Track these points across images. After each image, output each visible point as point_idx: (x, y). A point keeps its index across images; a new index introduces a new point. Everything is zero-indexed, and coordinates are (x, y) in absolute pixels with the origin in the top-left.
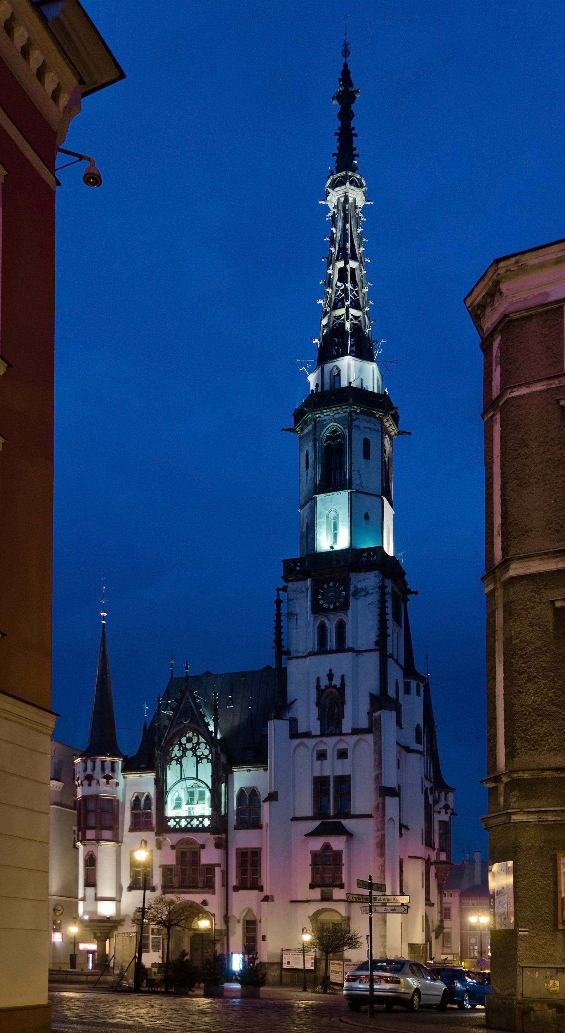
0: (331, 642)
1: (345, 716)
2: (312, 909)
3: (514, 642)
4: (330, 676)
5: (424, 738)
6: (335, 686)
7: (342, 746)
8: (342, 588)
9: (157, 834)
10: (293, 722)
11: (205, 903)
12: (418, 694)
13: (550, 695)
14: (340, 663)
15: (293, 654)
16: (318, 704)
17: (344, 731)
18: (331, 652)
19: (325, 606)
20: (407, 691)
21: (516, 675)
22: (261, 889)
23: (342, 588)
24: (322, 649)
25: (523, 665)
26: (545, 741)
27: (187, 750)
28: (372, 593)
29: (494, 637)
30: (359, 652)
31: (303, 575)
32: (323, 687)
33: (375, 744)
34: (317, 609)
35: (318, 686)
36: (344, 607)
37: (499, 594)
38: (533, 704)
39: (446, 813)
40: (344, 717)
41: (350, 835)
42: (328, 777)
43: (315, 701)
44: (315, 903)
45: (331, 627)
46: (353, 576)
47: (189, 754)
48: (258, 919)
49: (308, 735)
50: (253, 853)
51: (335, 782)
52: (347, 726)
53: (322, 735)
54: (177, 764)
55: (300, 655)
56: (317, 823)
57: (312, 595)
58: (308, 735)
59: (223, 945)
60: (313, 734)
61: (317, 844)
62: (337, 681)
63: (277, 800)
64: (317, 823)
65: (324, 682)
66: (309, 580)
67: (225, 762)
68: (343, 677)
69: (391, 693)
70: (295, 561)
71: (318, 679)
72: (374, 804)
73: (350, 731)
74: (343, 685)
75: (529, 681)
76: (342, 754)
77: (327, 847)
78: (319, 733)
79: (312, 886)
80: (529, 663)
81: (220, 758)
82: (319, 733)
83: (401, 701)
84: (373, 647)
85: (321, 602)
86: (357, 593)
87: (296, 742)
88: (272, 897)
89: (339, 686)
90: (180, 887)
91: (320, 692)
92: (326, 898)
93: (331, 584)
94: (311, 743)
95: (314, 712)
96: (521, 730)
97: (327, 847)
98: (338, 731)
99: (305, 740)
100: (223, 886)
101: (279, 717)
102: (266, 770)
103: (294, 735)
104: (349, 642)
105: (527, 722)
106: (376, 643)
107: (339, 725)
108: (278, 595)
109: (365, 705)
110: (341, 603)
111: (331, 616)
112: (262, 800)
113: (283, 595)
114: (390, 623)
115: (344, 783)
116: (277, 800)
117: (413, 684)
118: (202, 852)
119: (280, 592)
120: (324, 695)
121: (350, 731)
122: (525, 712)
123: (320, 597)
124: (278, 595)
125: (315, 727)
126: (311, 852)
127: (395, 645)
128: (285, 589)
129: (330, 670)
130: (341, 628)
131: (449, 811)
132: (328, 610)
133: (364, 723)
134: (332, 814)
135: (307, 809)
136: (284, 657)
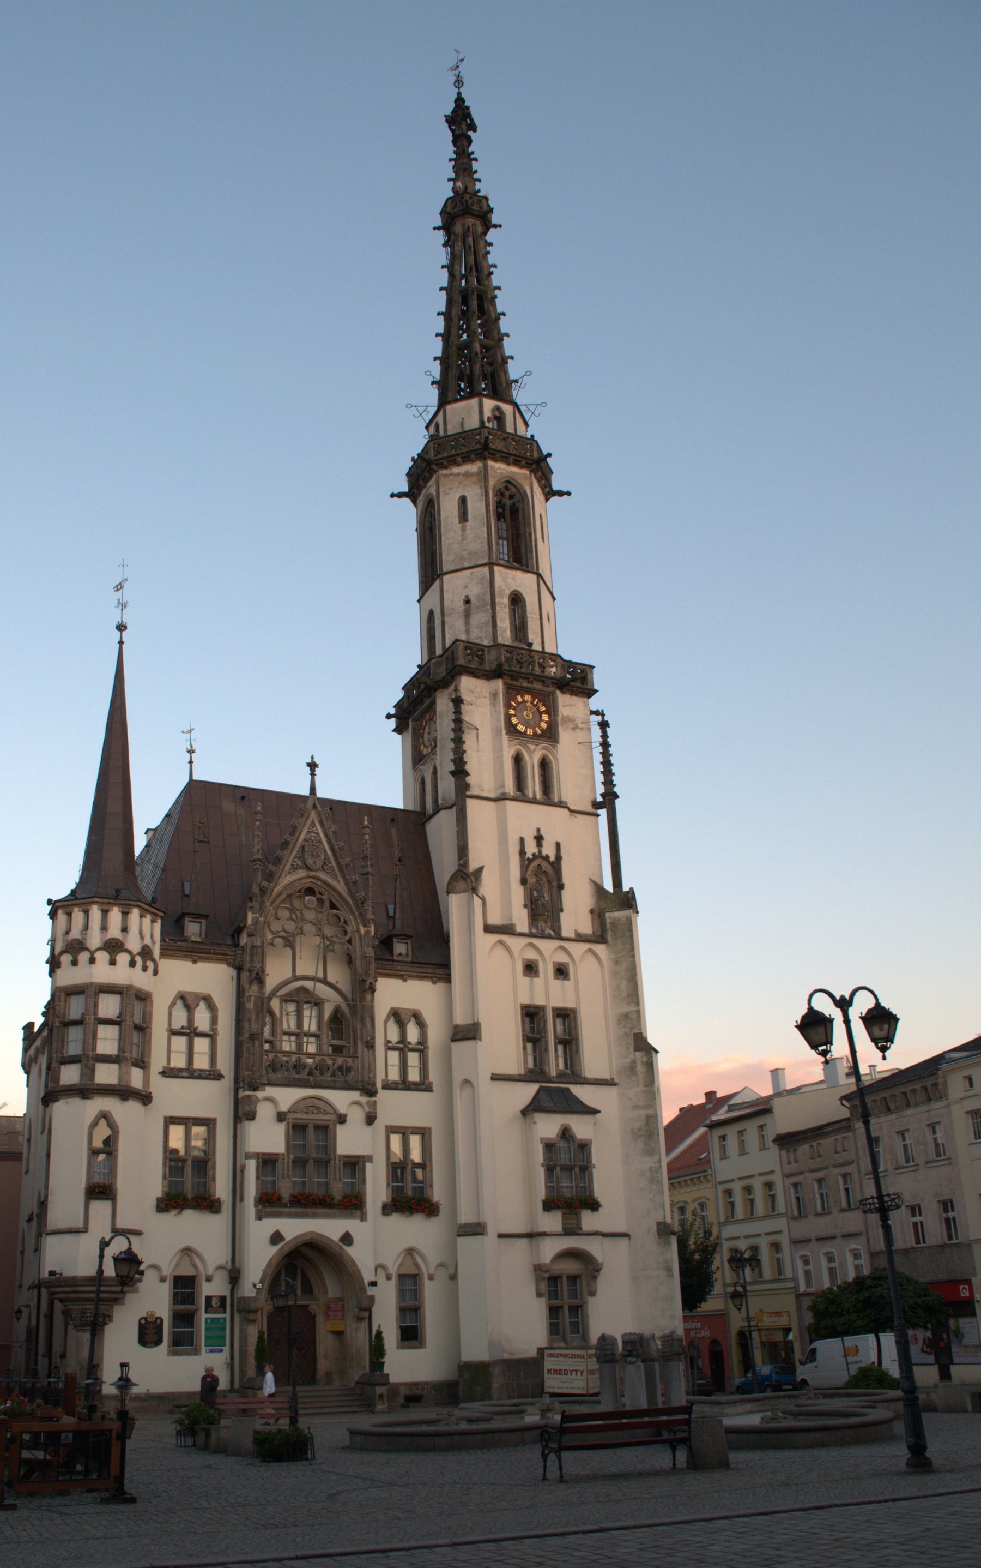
0: (534, 786)
1: (564, 907)
2: (549, 1249)
4: (539, 839)
6: (547, 858)
7: (562, 958)
11: (347, 1239)
16: (524, 881)
17: (564, 934)
18: (534, 801)
24: (521, 794)
28: (582, 729)
30: (571, 811)
32: (529, 855)
33: (616, 962)
34: (512, 730)
35: (522, 852)
36: (550, 735)
40: (562, 910)
44: (554, 1238)
49: (507, 930)
53: (531, 935)
54: (286, 946)
55: (485, 794)
56: (531, 1089)
58: (507, 930)
61: (548, 1126)
64: (533, 1088)
68: (558, 845)
71: (522, 840)
74: (559, 858)
76: (561, 972)
77: (566, 1133)
79: (548, 1206)
82: (526, 930)
85: (514, 720)
89: (552, 858)
91: (525, 862)
92: (571, 1230)
93: (528, 698)
94: (516, 944)
95: (518, 894)
97: (566, 1133)
99: (506, 939)
110: (542, 730)
118: (341, 1130)
120: (531, 868)
121: (572, 935)
125: (521, 920)
129: (538, 830)
134: (553, 1073)
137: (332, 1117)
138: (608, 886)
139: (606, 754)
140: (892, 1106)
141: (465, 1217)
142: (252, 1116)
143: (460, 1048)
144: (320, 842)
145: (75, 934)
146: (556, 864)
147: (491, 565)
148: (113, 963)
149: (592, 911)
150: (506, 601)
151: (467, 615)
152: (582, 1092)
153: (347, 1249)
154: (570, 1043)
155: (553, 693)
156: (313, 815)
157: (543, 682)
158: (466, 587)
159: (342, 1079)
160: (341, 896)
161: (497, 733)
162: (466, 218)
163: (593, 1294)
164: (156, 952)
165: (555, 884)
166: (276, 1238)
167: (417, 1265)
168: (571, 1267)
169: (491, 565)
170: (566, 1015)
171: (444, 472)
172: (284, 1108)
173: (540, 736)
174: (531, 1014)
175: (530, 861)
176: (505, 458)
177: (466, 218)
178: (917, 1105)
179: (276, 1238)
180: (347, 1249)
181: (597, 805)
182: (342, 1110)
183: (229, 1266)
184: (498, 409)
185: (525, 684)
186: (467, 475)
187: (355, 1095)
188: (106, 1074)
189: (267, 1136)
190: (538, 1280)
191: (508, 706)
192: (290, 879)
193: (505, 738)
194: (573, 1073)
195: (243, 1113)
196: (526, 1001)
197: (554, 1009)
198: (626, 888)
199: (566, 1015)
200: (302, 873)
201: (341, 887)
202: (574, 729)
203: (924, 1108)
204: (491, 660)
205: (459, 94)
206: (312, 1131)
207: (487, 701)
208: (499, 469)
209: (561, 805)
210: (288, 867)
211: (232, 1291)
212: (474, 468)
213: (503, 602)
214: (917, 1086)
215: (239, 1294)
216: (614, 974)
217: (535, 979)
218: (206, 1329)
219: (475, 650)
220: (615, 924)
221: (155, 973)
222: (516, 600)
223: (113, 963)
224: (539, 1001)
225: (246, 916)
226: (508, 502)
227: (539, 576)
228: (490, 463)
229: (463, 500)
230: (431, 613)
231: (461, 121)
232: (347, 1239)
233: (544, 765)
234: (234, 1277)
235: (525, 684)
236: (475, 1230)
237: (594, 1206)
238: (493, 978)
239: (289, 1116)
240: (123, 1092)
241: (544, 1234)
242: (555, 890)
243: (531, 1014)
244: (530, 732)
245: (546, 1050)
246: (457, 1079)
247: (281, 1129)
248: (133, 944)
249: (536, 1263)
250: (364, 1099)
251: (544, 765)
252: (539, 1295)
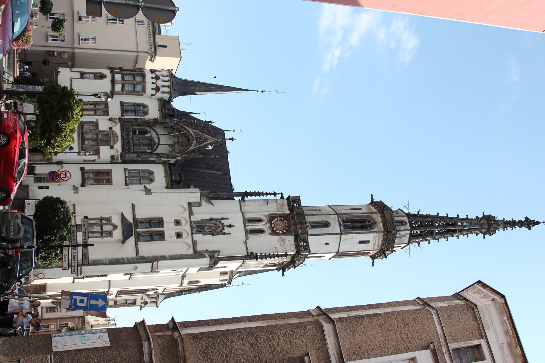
3: (278, 331)
4: (230, 226)
5: (193, 286)
6: (224, 229)
7: (184, 235)
8: (285, 231)
9: (119, 119)
10: (199, 204)
12: (221, 280)
13: (242, 360)
14: (238, 231)
15: (242, 203)
16: (211, 219)
17: (194, 235)
18: (245, 226)
19: (273, 222)
20: (222, 273)
21: (255, 335)
22: (83, 185)
23: (285, 231)
25: (262, 339)
26: (207, 360)
27: (178, 139)
29: (280, 318)
31: (291, 209)
32: (222, 222)
33: (187, 255)
34: (271, 217)
35: (223, 219)
36: (274, 233)
37: (310, 319)
38: (234, 349)
39: (142, 303)
41: (123, 242)
42: (162, 226)
43: (213, 217)
45: (260, 226)
46: (292, 238)
47: (176, 140)
48: (61, 184)
49: (191, 213)
50: (109, 179)
51: (160, 231)
52: (198, 237)
53: (191, 222)
55: (242, 207)
56: (131, 220)
57: (280, 214)
58: (191, 213)
59: (41, 161)
60: (192, 217)
61: (117, 220)
62: (226, 230)
63: (146, 194)
64: (131, 220)
65: (225, 222)
66: (289, 212)
67: (171, 162)
68: (230, 234)
69: (220, 264)
70: (299, 203)
71: (228, 219)
73: (194, 239)
74: (224, 234)
75: (251, 345)
76: (179, 235)
77: (115, 227)
78: (192, 220)
80: (264, 343)
81: (173, 158)
82: (192, 220)
83: (215, 270)
84: (249, 251)
85: (276, 219)
86: (283, 240)
87: (186, 206)
88: (78, 193)
89: (224, 231)
91: (220, 220)
93: (287, 225)
94: (186, 215)
95: (207, 217)
96: (214, 343)
98: (194, 232)
99: (187, 211)
100: (84, 161)
101: (202, 195)
102: (167, 188)
103: (190, 204)
104: (252, 237)
105: (221, 346)
106: (252, 253)
107: (198, 232)
108: (279, 194)
109: (211, 248)
111: (267, 225)
112: (146, 185)
113: (278, 197)
114: (265, 261)
115: (161, 236)
116: (146, 194)
117: (227, 277)
119: (280, 195)
120: (217, 223)
121: (194, 239)
122: (228, 344)
123: (279, 218)
124: (279, 194)
125: (196, 218)
126: (111, 217)
127: (251, 265)
128: (282, 197)
129: (233, 226)
130: (261, 231)
131: (143, 305)
132: (271, 223)
133: (200, 248)
134: (138, 230)
135: (141, 214)
136: (240, 198)
145: (161, 78)
146: (222, 233)
150: (324, 220)
152: (131, 241)
156: (215, 139)
162: (488, 225)
164: (159, 95)
169: (337, 214)
172: (114, 129)
173: (273, 230)
174: (160, 222)
175: (220, 222)
176: (383, 217)
177: (488, 225)
182: (114, 146)
184: (406, 223)
187: (120, 150)
188: (118, 77)
192: (191, 132)
193: (266, 214)
196: (165, 220)
197: (163, 231)
199: (161, 236)
201: (192, 148)
202: (281, 245)
205: (541, 223)
208: (377, 217)
212: (375, 210)
217: (174, 224)
221: (152, 95)
222: (327, 225)
223: (152, 78)
224: (165, 225)
226: (367, 223)
227: (341, 234)
231: (529, 224)
233: (261, 231)
240: (113, 82)
243: (160, 222)
247: (107, 129)
248: (160, 83)
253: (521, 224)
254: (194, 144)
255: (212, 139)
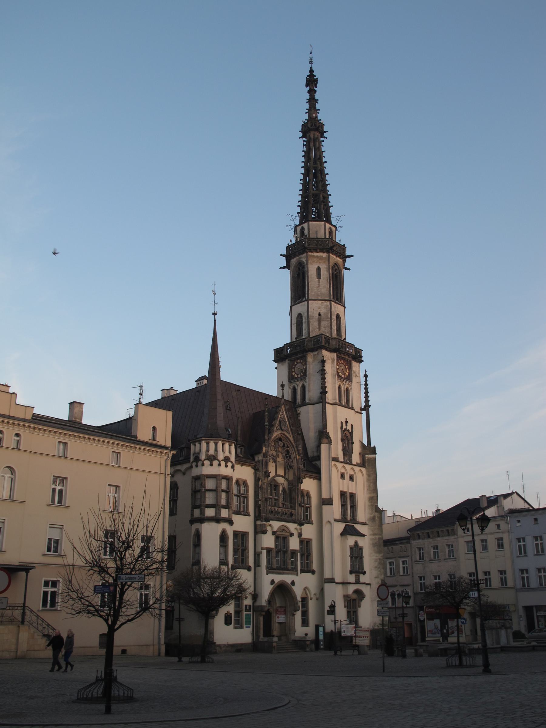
2: (351, 589)
4: (346, 422)
7: (352, 473)
11: (293, 583)
16: (342, 440)
17: (354, 462)
30: (356, 412)
33: (369, 475)
35: (342, 428)
45: (343, 389)
49: (336, 459)
58: (336, 459)
61: (351, 540)
68: (352, 426)
71: (342, 423)
72: (368, 516)
76: (351, 478)
77: (356, 543)
79: (351, 573)
90: (278, 569)
92: (358, 582)
94: (340, 465)
97: (356, 543)
121: (355, 464)
137: (288, 534)
138: (365, 443)
139: (366, 389)
140: (431, 536)
141: (327, 575)
142: (265, 532)
143: (325, 508)
144: (285, 419)
146: (351, 433)
147: (330, 301)
148: (226, 466)
149: (360, 454)
150: (335, 318)
151: (319, 321)
153: (293, 587)
154: (353, 507)
155: (351, 361)
157: (349, 356)
158: (319, 308)
159: (290, 519)
160: (291, 443)
161: (334, 376)
162: (313, 130)
163: (360, 606)
165: (350, 442)
166: (272, 582)
167: (306, 594)
168: (355, 596)
170: (353, 495)
171: (310, 253)
172: (275, 529)
177: (313, 130)
178: (443, 536)
179: (272, 582)
180: (293, 587)
181: (362, 409)
183: (253, 593)
184: (330, 228)
185: (343, 356)
186: (321, 258)
189: (269, 541)
190: (345, 601)
191: (337, 365)
193: (337, 378)
194: (354, 520)
195: (259, 530)
197: (350, 493)
198: (372, 446)
199: (353, 495)
200: (280, 432)
201: (291, 439)
203: (447, 538)
204: (333, 344)
205: (311, 68)
206: (282, 538)
207: (330, 362)
209: (352, 408)
210: (275, 429)
211: (253, 603)
212: (324, 255)
213: (334, 317)
214: (444, 529)
215: (257, 604)
216: (368, 480)
218: (246, 618)
219: (328, 340)
220: (369, 459)
222: (338, 317)
224: (345, 490)
225: (262, 448)
228: (331, 255)
229: (319, 269)
230: (300, 316)
231: (312, 81)
232: (293, 583)
233: (347, 390)
234: (255, 597)
235: (343, 356)
236: (331, 581)
237: (364, 573)
238: (335, 479)
239: (277, 533)
241: (350, 583)
242: (350, 444)
244: (343, 376)
245: (347, 509)
246: (325, 520)
247: (273, 538)
249: (345, 594)
250: (299, 527)
251: (347, 390)
252: (345, 607)
253: (312, 92)
254: (288, 435)
255: (283, 412)
